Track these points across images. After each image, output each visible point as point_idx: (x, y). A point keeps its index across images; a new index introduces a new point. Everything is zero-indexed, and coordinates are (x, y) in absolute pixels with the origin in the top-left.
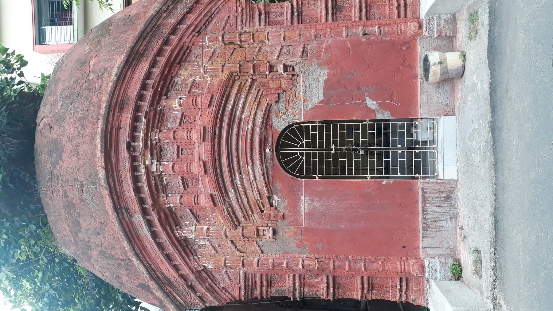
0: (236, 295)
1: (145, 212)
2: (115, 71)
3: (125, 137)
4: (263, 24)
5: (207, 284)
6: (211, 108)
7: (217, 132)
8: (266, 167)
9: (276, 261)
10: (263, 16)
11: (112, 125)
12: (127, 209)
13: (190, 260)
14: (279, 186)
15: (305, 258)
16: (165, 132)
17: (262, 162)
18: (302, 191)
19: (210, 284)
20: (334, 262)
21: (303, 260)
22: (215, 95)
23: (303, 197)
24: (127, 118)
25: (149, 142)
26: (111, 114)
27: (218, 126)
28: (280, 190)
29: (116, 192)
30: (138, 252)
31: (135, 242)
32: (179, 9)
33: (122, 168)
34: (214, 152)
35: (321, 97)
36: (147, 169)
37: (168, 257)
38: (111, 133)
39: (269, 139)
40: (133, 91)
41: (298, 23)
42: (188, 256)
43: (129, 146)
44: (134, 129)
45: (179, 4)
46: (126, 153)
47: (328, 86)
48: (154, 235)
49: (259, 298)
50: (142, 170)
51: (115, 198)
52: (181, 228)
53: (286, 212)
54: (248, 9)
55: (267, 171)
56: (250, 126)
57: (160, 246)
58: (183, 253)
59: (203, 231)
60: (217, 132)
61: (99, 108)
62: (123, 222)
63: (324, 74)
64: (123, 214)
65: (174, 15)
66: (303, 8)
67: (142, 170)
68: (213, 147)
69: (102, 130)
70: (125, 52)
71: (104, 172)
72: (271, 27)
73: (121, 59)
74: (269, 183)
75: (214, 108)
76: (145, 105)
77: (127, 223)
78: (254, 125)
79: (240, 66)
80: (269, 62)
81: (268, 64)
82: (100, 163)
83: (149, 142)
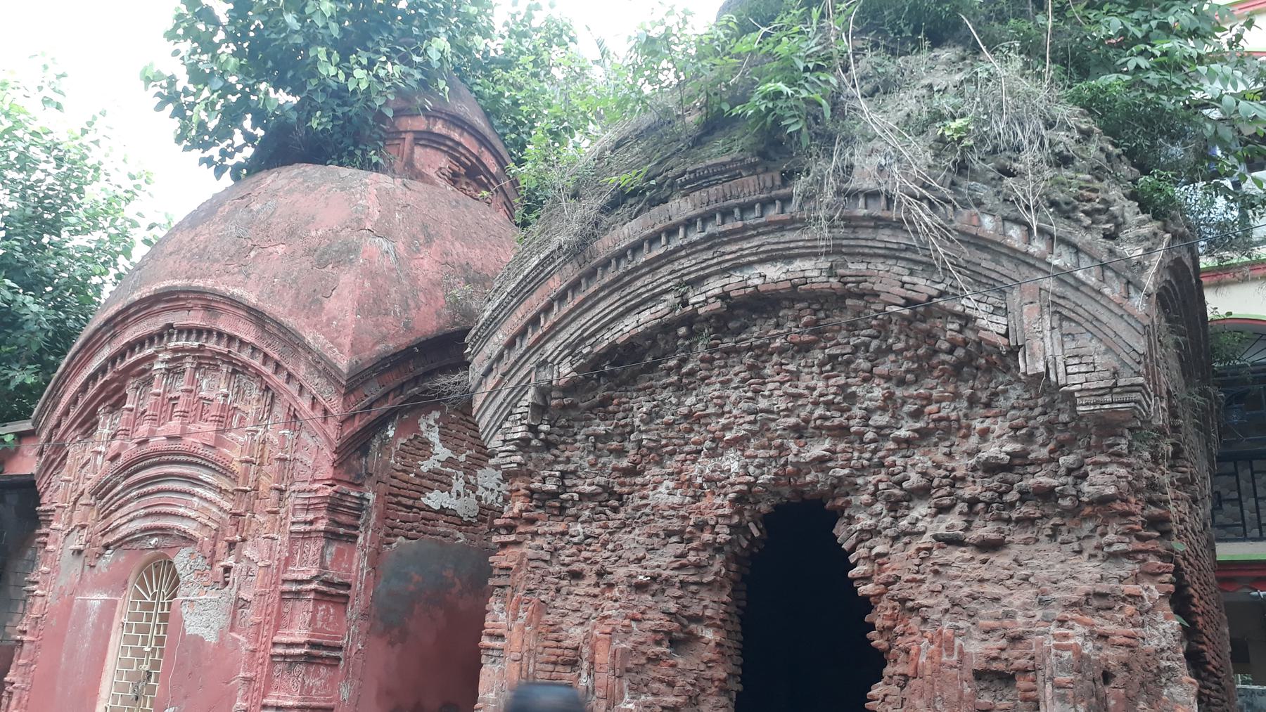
0: (45, 499)
1: (113, 360)
2: (237, 291)
3: (180, 319)
4: (295, 528)
5: (52, 457)
6: (200, 446)
7: (176, 458)
8: (141, 538)
9: (51, 555)
10: (308, 528)
11: (188, 299)
12: (114, 336)
13: (75, 430)
14: (122, 559)
15: (46, 598)
16: (194, 376)
17: (146, 530)
18: (111, 596)
19: (54, 460)
20: (32, 642)
21: (43, 596)
22: (214, 451)
23: (105, 597)
24: (195, 319)
25: (180, 354)
26: (196, 295)
27: (185, 458)
28: (117, 561)
29: (127, 318)
30: (77, 359)
31: (86, 353)
32: (317, 381)
33: (150, 321)
34: (161, 455)
35: (190, 631)
36: (152, 358)
37: (74, 401)
38: (178, 299)
39: (168, 542)
40: (224, 324)
41: (283, 593)
42: (81, 425)
43: (170, 326)
44: (188, 331)
45: (324, 381)
46: (161, 325)
47: (198, 640)
48: (93, 377)
49: (38, 531)
50: (148, 351)
51: (120, 318)
52: (111, 412)
53: (95, 571)
54: (316, 501)
55: (137, 540)
56: (181, 510)
57: (84, 388)
58: (80, 420)
59: (98, 446)
60: (179, 458)
61: (202, 277)
62: (99, 334)
63: (211, 638)
64: (109, 331)
65: (311, 373)
66: (303, 601)
67: (148, 351)
68: (162, 454)
69: (176, 286)
70: (260, 303)
71: (137, 298)
72: (286, 542)
73: (252, 299)
74: (126, 543)
75: (200, 451)
76: (211, 344)
77: (101, 337)
78: (183, 516)
79: (246, 491)
80: (244, 540)
81: (238, 538)
82: (146, 291)
83: (180, 354)
